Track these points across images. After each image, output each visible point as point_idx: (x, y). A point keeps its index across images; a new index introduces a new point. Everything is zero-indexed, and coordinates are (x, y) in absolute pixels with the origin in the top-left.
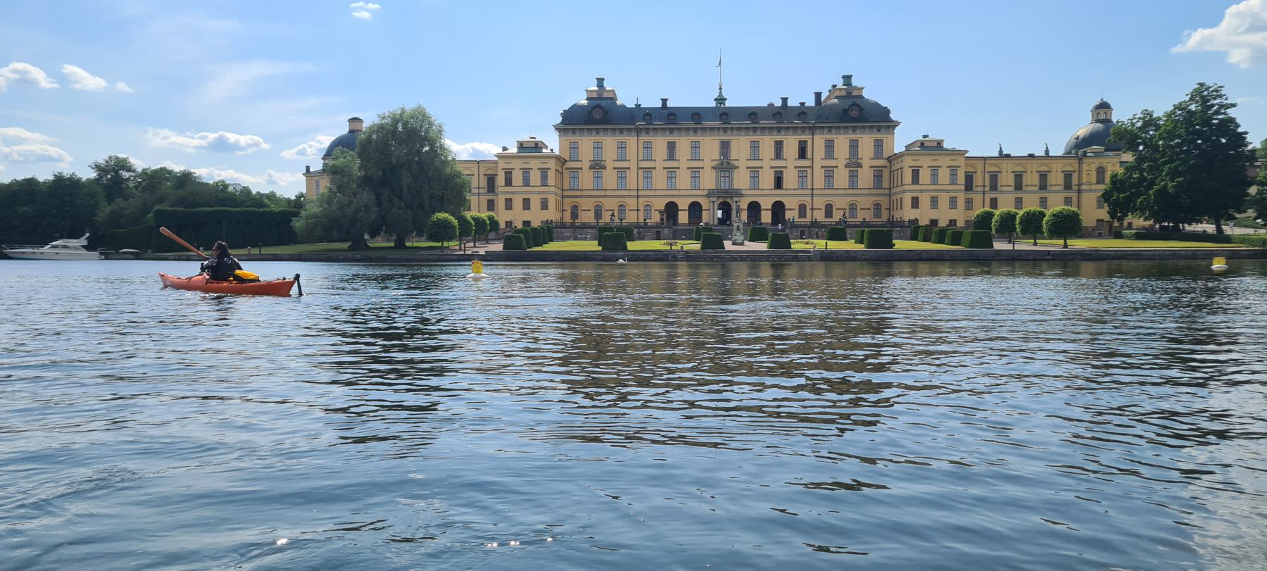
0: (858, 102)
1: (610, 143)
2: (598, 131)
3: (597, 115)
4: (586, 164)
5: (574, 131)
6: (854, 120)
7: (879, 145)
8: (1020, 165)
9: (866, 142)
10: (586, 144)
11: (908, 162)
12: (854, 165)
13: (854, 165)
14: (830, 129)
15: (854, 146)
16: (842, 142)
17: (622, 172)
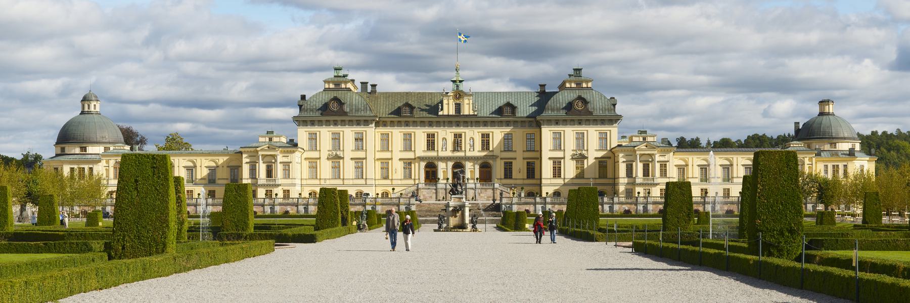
0: (586, 95)
1: (348, 133)
2: (335, 123)
3: (334, 107)
4: (324, 154)
5: (313, 123)
6: (579, 113)
7: (603, 138)
8: (727, 159)
9: (593, 133)
10: (325, 133)
11: (621, 158)
12: (580, 158)
13: (580, 158)
14: (557, 123)
15: (580, 138)
16: (569, 133)
17: (359, 163)
